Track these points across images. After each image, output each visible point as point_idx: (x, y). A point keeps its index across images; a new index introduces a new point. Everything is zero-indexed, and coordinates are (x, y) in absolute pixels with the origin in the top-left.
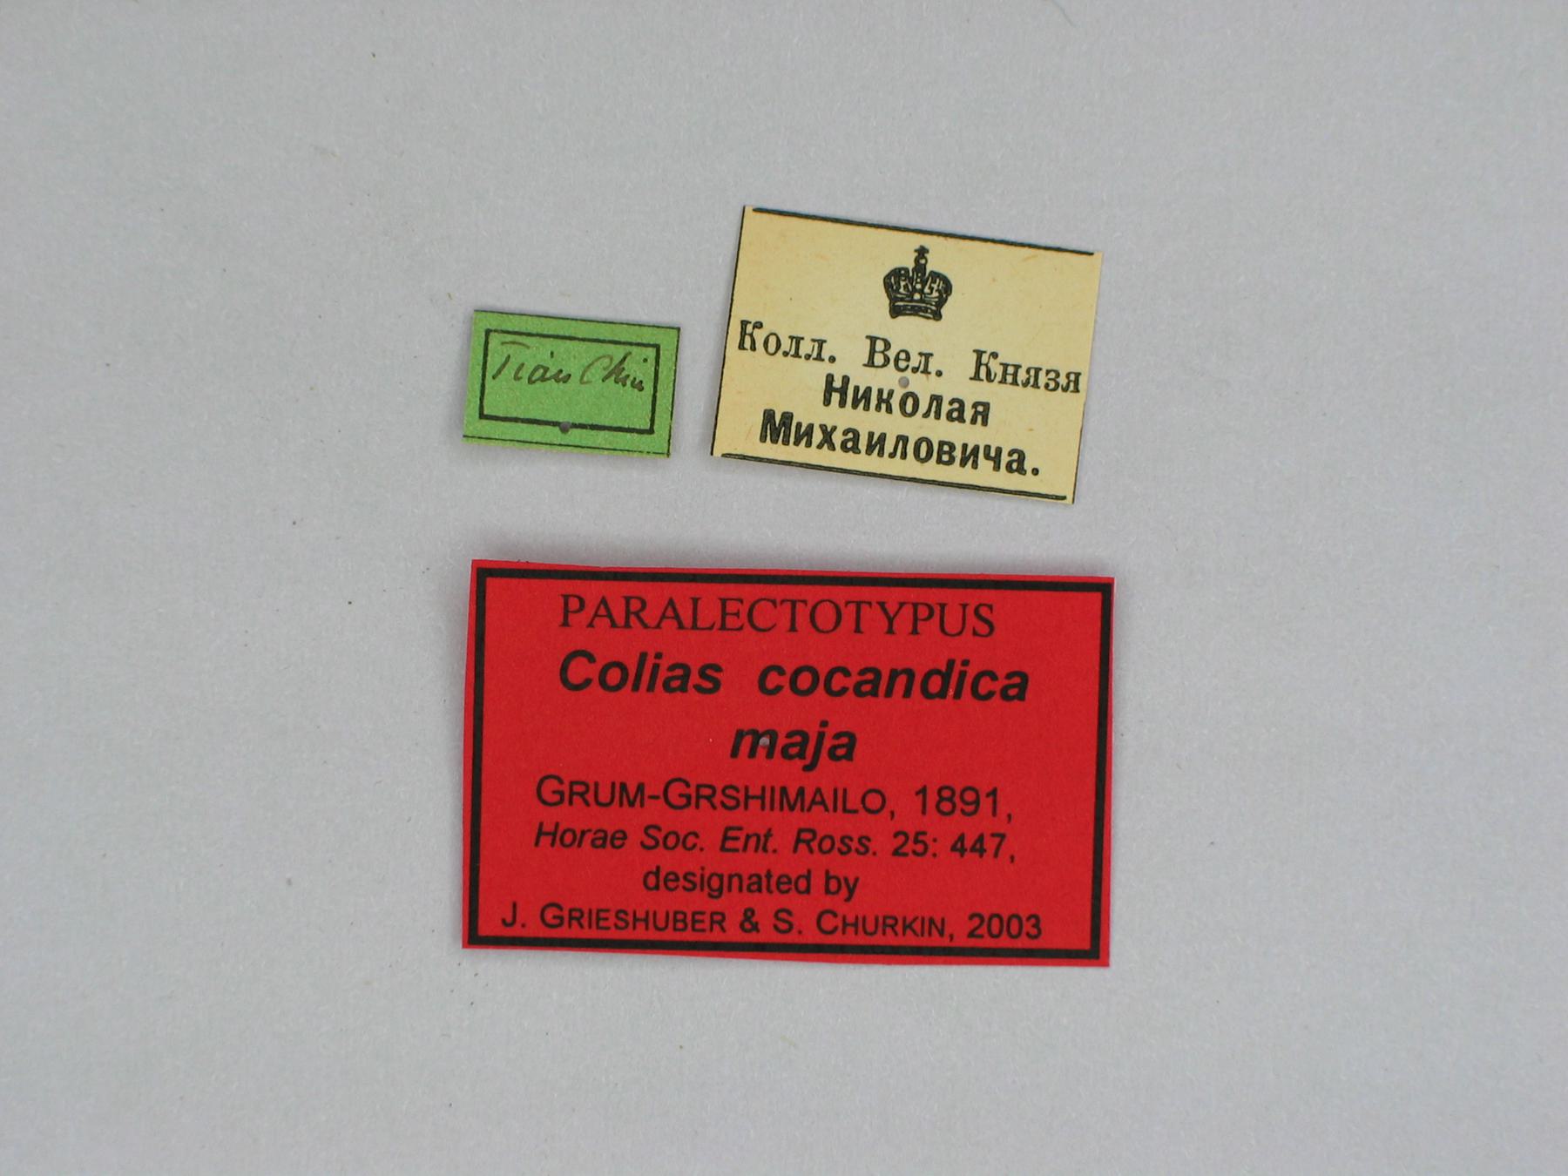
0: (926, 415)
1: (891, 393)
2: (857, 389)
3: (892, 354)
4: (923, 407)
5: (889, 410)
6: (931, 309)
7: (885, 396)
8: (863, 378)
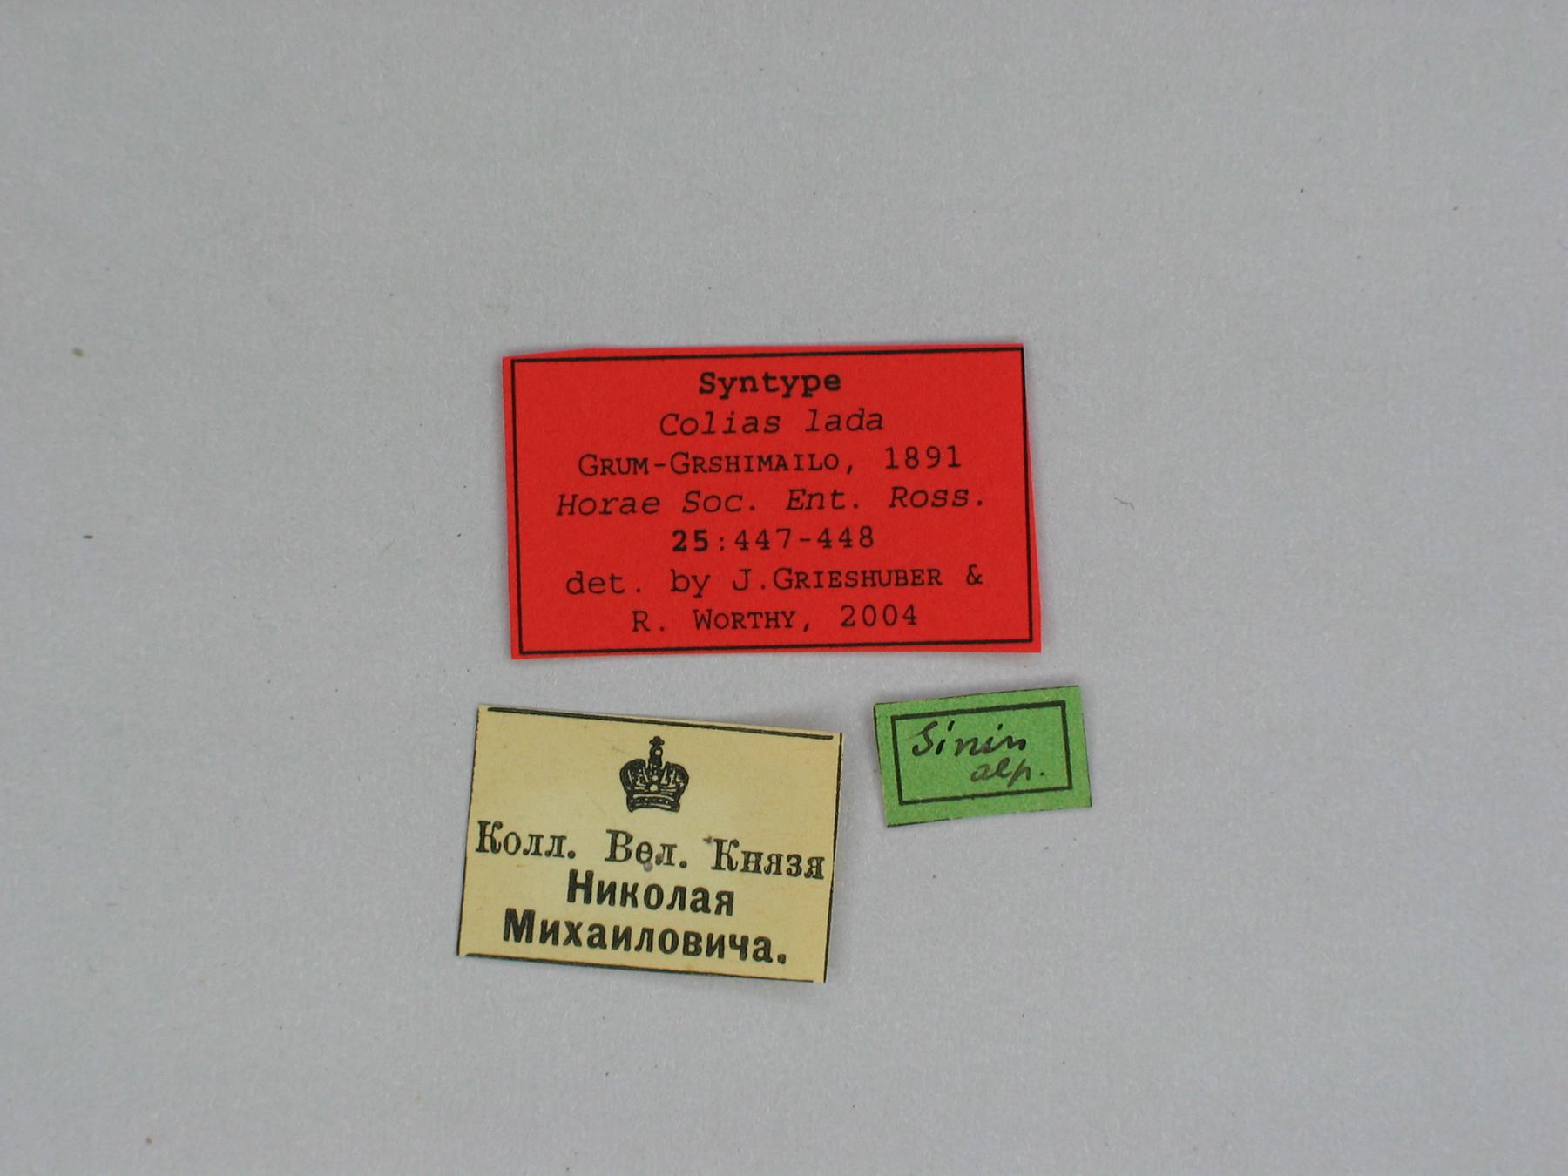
0: (670, 907)
1: (635, 887)
2: (601, 884)
3: (633, 846)
4: (667, 900)
5: (635, 903)
6: (667, 799)
7: (630, 889)
8: (608, 873)
